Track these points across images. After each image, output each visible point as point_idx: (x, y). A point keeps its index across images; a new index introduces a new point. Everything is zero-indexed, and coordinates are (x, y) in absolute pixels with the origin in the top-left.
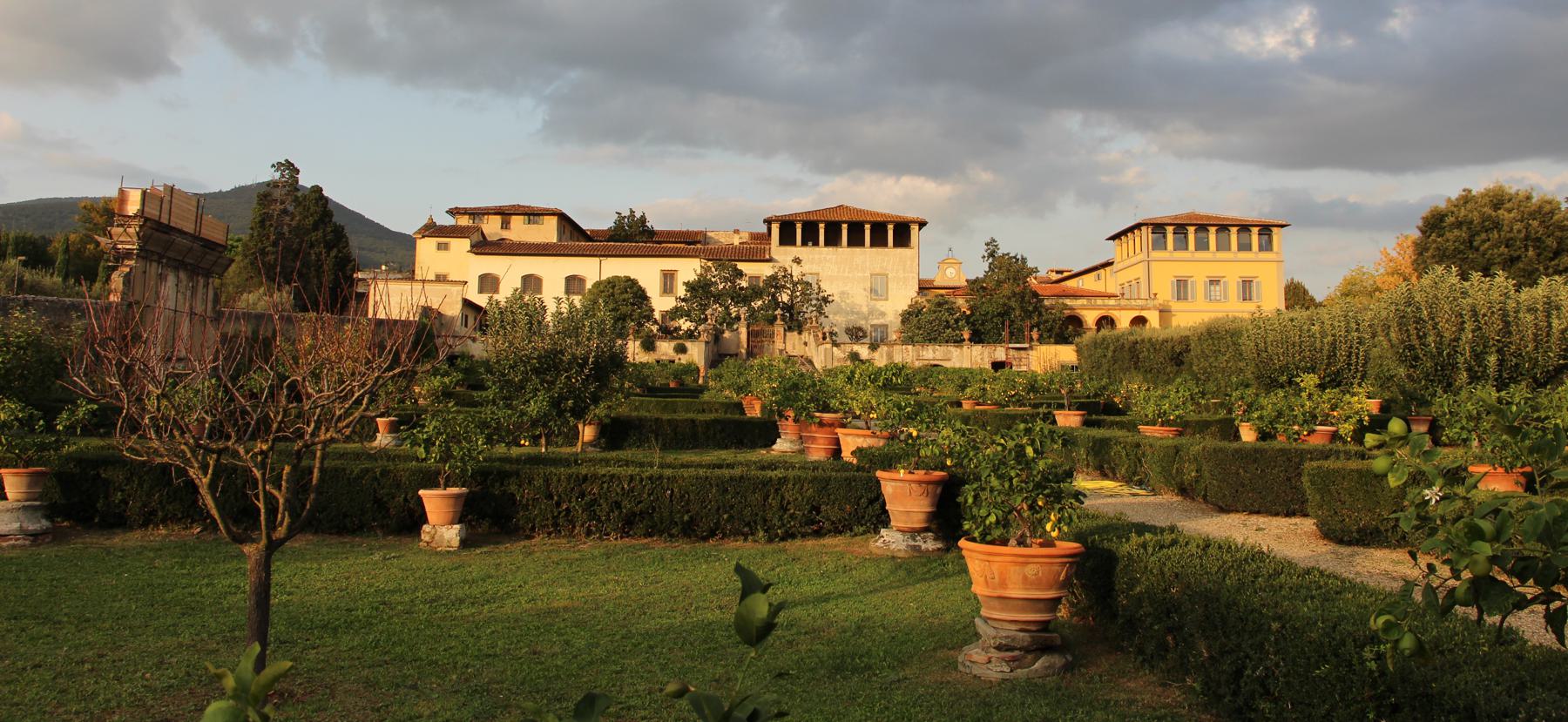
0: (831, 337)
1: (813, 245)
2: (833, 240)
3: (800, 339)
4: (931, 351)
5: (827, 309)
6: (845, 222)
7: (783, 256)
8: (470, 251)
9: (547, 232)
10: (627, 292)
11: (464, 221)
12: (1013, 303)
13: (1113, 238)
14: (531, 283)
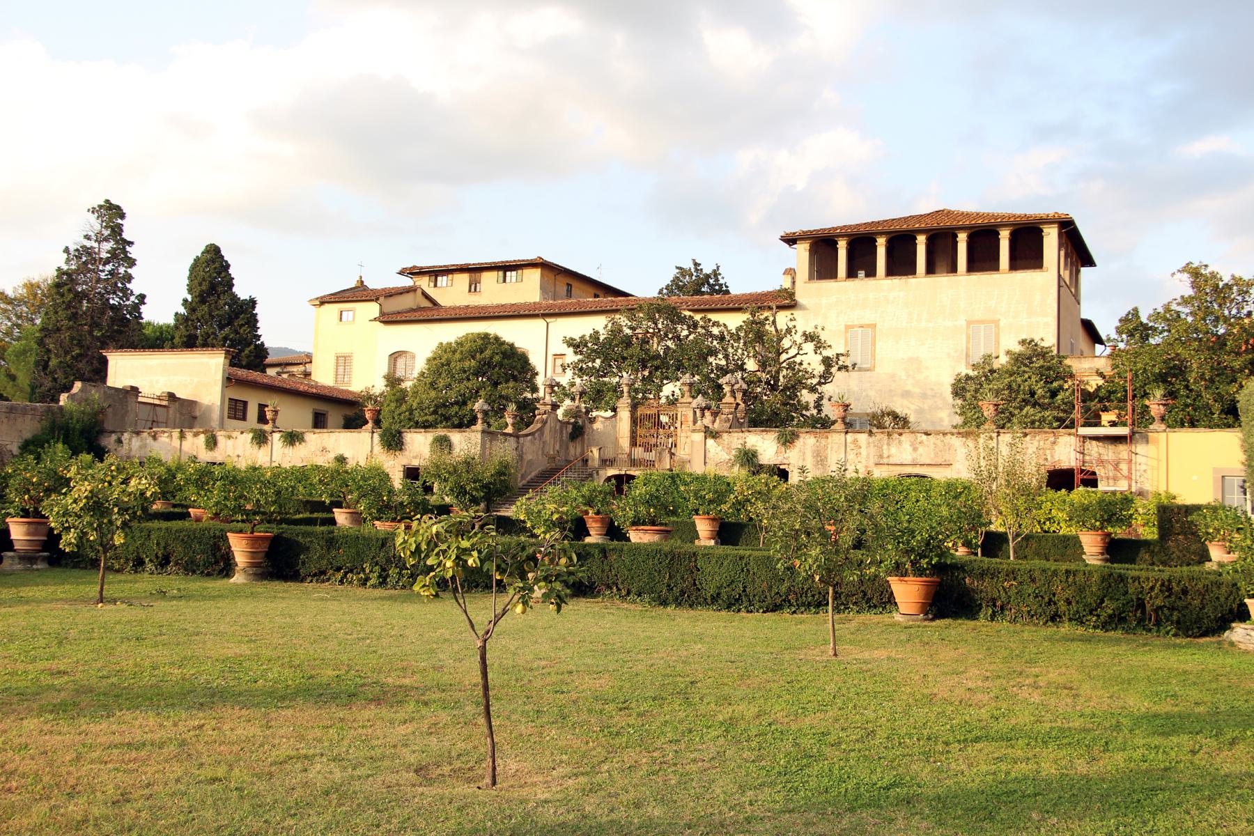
1: (867, 275)
2: (901, 264)
6: (921, 231)
10: (473, 357)
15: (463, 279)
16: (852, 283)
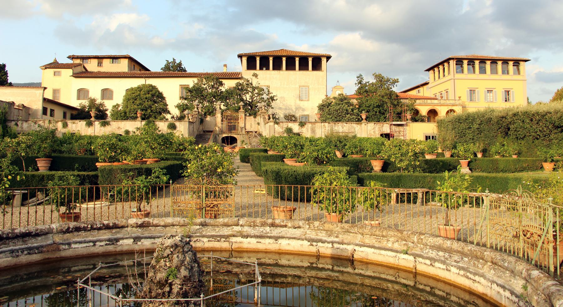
0: (275, 119)
1: (266, 69)
2: (277, 66)
3: (255, 121)
4: (340, 127)
5: (273, 104)
7: (248, 75)
8: (72, 76)
9: (123, 66)
10: (149, 94)
11: (78, 61)
12: (386, 99)
13: (429, 70)
14: (107, 93)
15: (96, 61)
16: (261, 72)
